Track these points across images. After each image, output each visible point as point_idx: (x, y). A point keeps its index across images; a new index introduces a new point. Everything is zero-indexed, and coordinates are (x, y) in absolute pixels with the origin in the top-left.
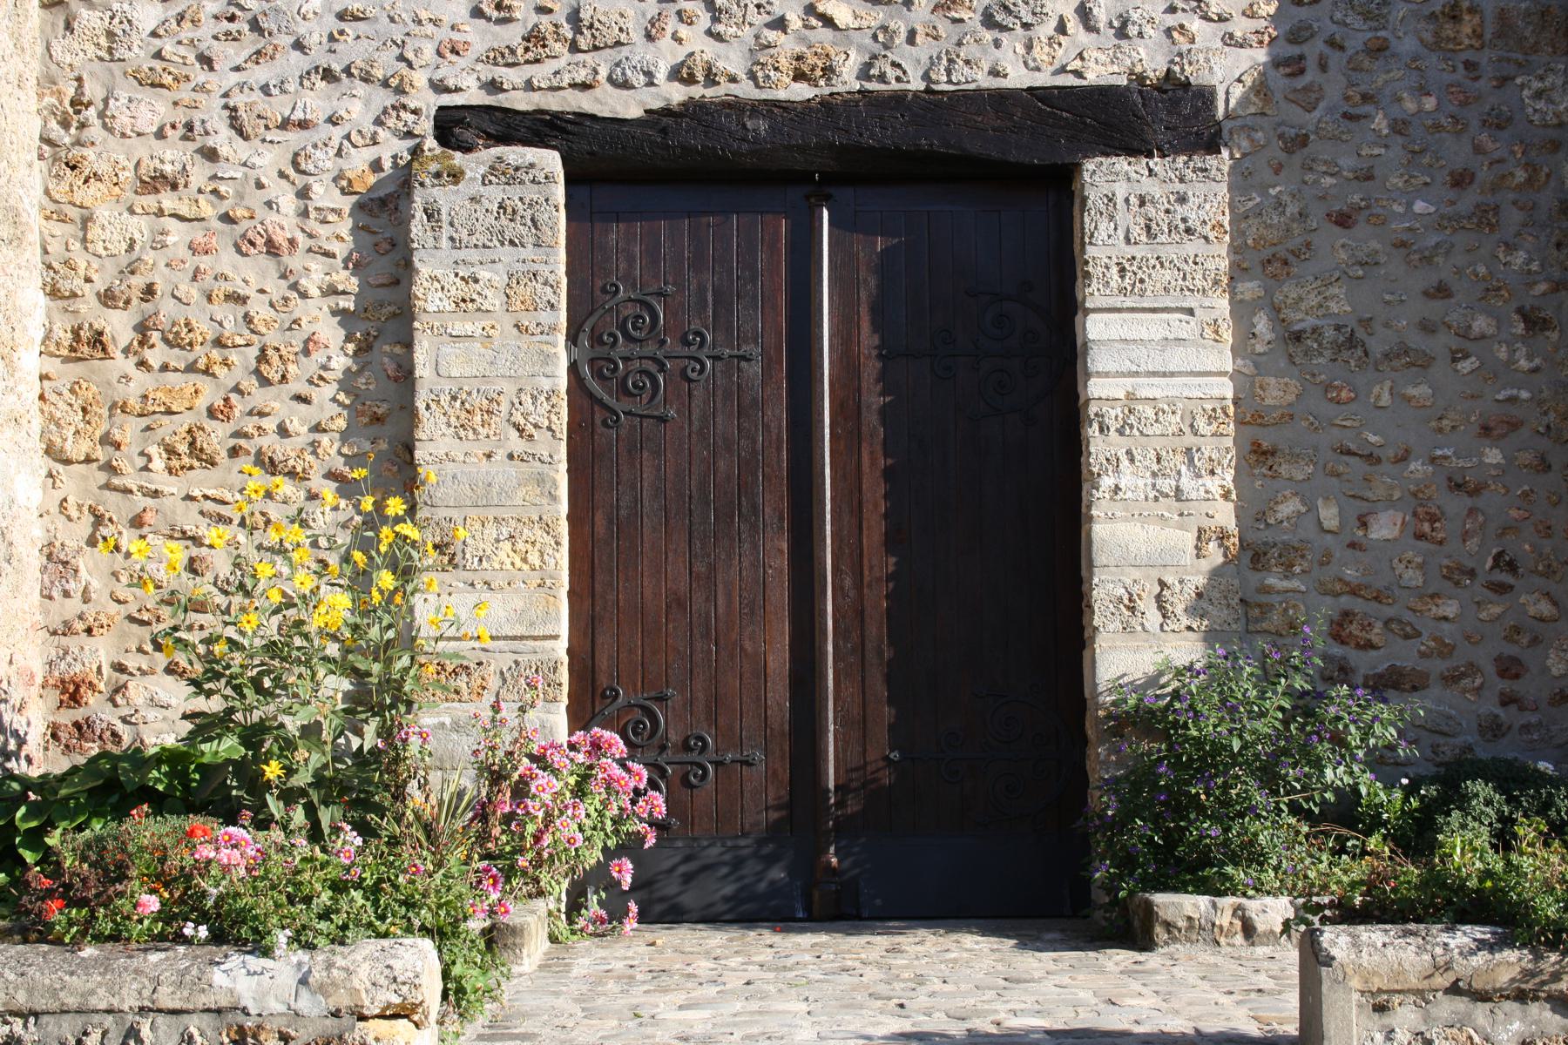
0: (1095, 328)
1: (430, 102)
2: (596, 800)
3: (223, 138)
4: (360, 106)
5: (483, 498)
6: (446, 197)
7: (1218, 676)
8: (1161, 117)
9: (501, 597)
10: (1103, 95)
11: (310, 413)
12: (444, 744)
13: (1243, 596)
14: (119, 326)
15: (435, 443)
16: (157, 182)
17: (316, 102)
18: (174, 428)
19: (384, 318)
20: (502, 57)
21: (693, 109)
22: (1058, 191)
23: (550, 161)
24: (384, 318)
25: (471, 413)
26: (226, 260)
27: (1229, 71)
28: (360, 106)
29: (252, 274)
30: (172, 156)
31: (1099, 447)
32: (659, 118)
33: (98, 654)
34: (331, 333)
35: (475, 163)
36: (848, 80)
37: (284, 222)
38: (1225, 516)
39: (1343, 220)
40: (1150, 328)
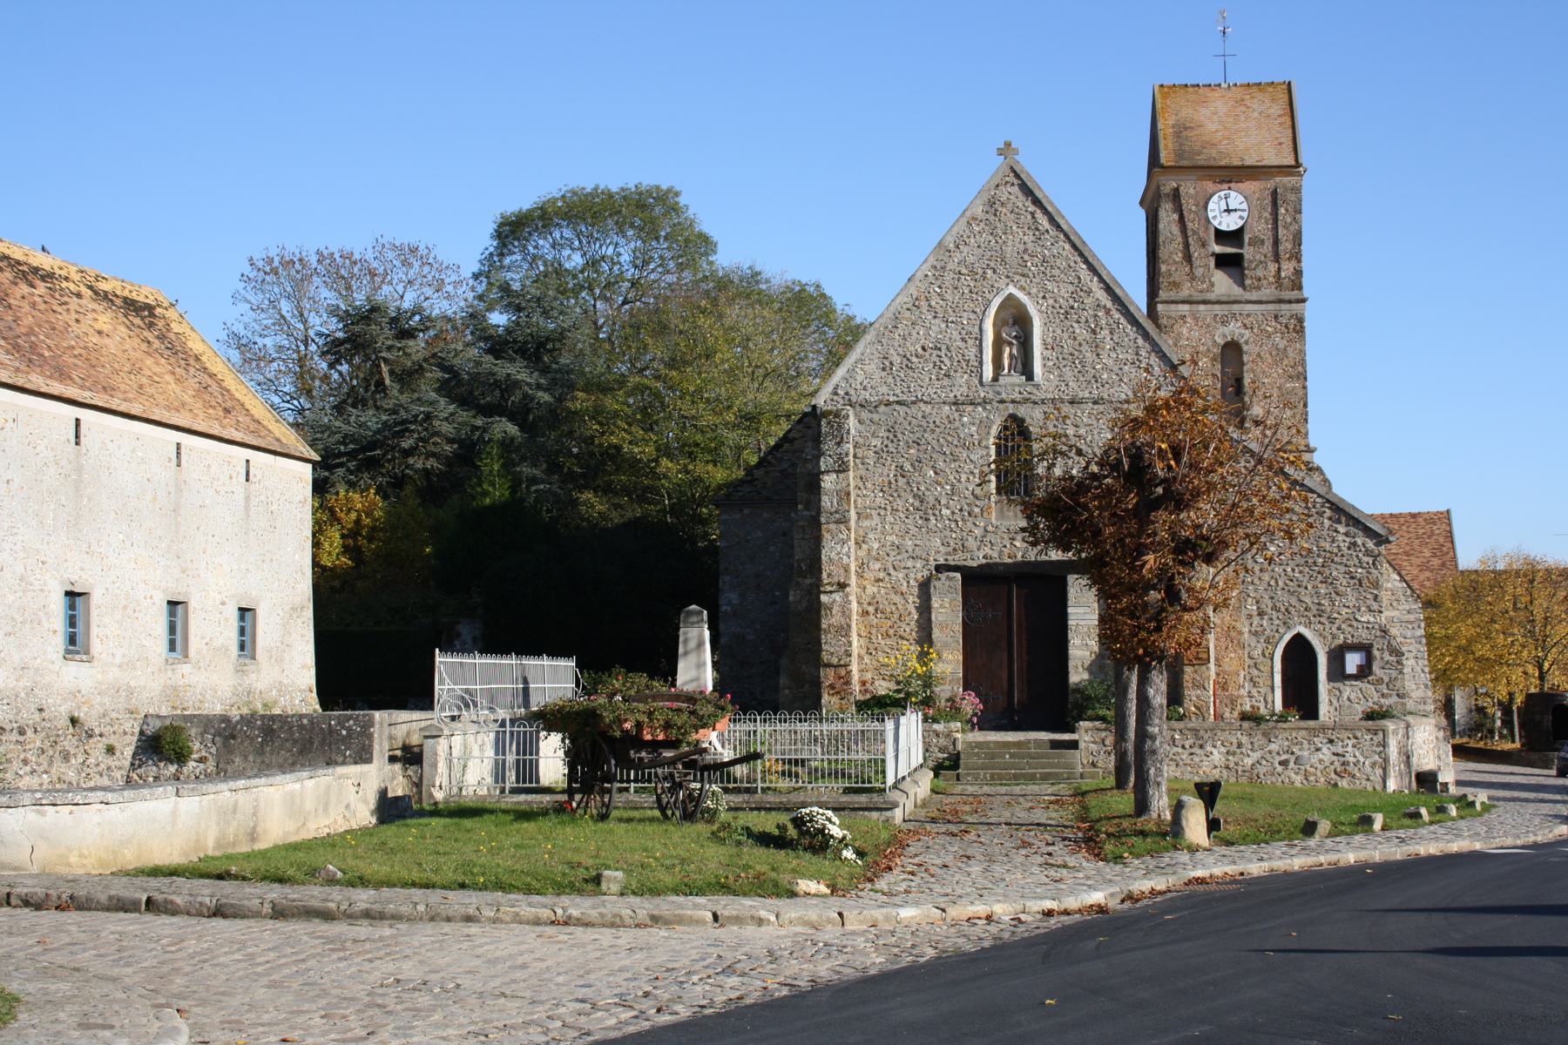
0: (1070, 610)
1: (933, 563)
2: (971, 704)
3: (892, 571)
4: (919, 565)
5: (946, 645)
6: (938, 584)
7: (1090, 682)
9: (949, 663)
11: (910, 628)
12: (943, 691)
13: (1096, 667)
14: (871, 609)
15: (936, 634)
16: (879, 580)
17: (910, 564)
18: (883, 630)
19: (925, 608)
20: (948, 554)
21: (987, 565)
23: (958, 575)
24: (925, 608)
25: (942, 627)
26: (893, 596)
28: (919, 565)
29: (897, 599)
30: (882, 575)
31: (1070, 635)
32: (980, 566)
33: (869, 676)
34: (914, 611)
35: (943, 576)
36: (1019, 558)
37: (904, 588)
38: (1096, 649)
40: (1081, 610)
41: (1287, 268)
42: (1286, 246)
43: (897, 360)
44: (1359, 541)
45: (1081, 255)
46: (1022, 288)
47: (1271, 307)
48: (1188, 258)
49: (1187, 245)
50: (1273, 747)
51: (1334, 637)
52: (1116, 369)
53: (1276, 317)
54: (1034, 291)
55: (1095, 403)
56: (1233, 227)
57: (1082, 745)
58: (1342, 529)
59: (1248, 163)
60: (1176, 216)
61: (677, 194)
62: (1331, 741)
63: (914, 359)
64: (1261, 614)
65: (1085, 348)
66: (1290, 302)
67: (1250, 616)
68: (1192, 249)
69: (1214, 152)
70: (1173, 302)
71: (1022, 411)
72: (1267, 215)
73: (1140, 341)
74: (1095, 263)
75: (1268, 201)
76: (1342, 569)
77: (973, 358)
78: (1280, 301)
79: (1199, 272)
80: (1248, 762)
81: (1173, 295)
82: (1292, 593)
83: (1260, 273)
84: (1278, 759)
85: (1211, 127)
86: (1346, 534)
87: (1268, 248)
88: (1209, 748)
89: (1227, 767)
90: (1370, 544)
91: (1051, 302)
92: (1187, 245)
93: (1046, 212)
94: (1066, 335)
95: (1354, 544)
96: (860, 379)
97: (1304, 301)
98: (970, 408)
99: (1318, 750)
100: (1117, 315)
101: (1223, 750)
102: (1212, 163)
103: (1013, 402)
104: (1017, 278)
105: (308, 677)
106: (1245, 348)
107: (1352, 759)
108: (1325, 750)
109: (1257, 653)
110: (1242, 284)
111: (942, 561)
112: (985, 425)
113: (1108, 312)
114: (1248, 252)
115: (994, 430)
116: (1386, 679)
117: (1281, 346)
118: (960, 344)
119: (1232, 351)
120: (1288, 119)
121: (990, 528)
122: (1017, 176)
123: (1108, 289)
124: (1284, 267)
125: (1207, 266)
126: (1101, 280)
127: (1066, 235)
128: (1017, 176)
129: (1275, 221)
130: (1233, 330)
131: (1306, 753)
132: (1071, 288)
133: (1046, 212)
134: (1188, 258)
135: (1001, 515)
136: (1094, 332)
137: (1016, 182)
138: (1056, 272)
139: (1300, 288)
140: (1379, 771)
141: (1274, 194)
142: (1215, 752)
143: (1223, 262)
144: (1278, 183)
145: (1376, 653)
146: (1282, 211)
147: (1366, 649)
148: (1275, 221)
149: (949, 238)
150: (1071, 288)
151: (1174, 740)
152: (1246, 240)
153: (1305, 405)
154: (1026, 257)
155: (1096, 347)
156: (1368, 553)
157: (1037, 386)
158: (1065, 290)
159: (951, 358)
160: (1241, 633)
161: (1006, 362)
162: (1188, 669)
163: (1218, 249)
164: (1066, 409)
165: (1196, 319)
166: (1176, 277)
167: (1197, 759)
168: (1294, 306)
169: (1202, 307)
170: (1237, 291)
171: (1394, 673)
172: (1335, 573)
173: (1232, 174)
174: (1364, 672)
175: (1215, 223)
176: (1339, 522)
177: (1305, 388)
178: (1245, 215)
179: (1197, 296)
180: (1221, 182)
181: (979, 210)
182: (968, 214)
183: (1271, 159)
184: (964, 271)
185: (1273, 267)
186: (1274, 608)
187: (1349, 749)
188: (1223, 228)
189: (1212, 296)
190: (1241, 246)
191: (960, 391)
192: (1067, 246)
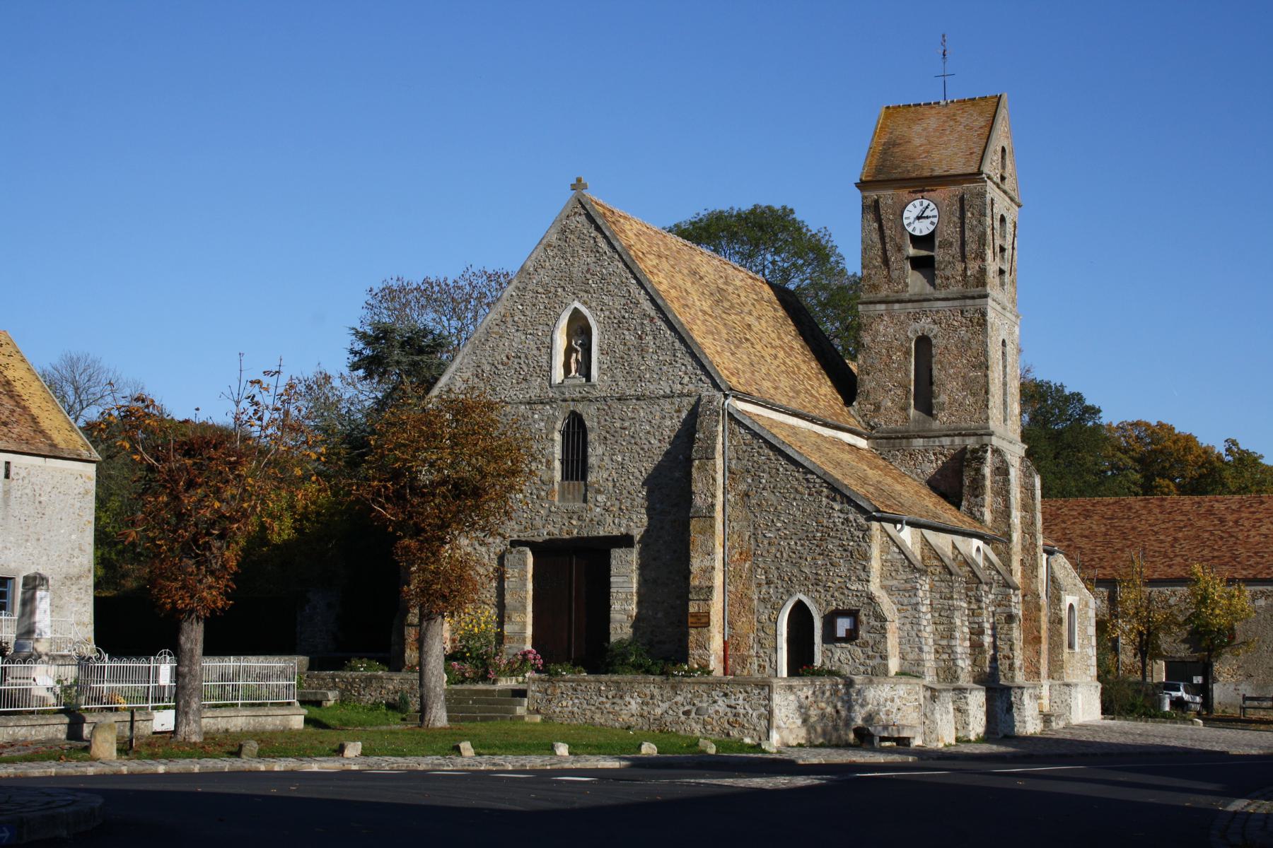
0: (612, 579)
3: (477, 546)
8: (625, 541)
10: (616, 537)
20: (520, 531)
27: (637, 533)
32: (545, 542)
39: (654, 559)
40: (621, 579)
41: (973, 267)
42: (972, 246)
43: (487, 368)
44: (851, 517)
45: (632, 272)
46: (585, 303)
47: (957, 303)
48: (886, 262)
49: (885, 251)
50: (679, 699)
51: (828, 603)
52: (656, 369)
53: (962, 312)
54: (594, 304)
55: (638, 399)
56: (925, 232)
57: (530, 694)
58: (837, 507)
59: (936, 173)
60: (876, 225)
61: (792, 211)
62: (726, 695)
63: (501, 367)
64: (769, 583)
65: (633, 352)
66: (973, 298)
67: (759, 585)
68: (889, 254)
69: (910, 166)
70: (871, 303)
71: (580, 408)
72: (956, 219)
73: (677, 344)
74: (642, 278)
75: (957, 207)
76: (837, 542)
77: (545, 364)
78: (965, 298)
79: (895, 274)
80: (658, 711)
81: (872, 296)
82: (794, 564)
83: (948, 272)
84: (682, 709)
85: (917, 142)
86: (841, 511)
87: (956, 249)
88: (627, 699)
89: (642, 716)
90: (862, 520)
91: (607, 313)
92: (885, 251)
93: (605, 237)
94: (618, 342)
95: (847, 520)
96: (458, 384)
97: (986, 296)
98: (540, 407)
99: (715, 702)
100: (659, 323)
101: (639, 700)
102: (905, 176)
103: (573, 400)
104: (582, 294)
105: (89, 632)
106: (934, 341)
107: (742, 711)
108: (720, 702)
109: (764, 617)
110: (932, 284)
111: (515, 537)
112: (551, 420)
113: (652, 319)
114: (938, 254)
115: (559, 425)
116: (871, 642)
117: (966, 338)
118: (535, 352)
119: (924, 343)
120: (987, 130)
121: (553, 509)
122: (583, 207)
123: (653, 301)
125: (902, 269)
126: (647, 293)
127: (620, 255)
128: (583, 207)
130: (925, 325)
131: (705, 705)
132: (623, 301)
133: (605, 237)
135: (563, 497)
136: (640, 338)
137: (583, 212)
138: (611, 288)
139: (984, 285)
140: (764, 723)
141: (962, 200)
142: (633, 702)
143: (917, 263)
144: (963, 188)
146: (969, 215)
147: (853, 614)
148: (963, 224)
149: (529, 263)
150: (623, 301)
151: (600, 690)
152: (937, 243)
153: (987, 392)
154: (588, 276)
155: (642, 351)
156: (859, 528)
157: (593, 386)
158: (618, 303)
159: (528, 365)
160: (751, 600)
161: (573, 367)
162: (692, 631)
163: (911, 251)
164: (616, 405)
165: (892, 317)
166: (875, 280)
167: (617, 708)
168: (978, 301)
169: (897, 306)
170: (929, 289)
171: (878, 637)
172: (830, 546)
173: (923, 184)
174: (852, 636)
175: (910, 229)
176: (834, 500)
177: (986, 376)
178: (935, 220)
179: (893, 296)
180: (915, 192)
181: (554, 238)
182: (544, 242)
183: (959, 168)
184: (541, 290)
185: (960, 267)
186: (780, 578)
187: (741, 702)
188: (917, 233)
189: (906, 296)
190: (932, 250)
191: (534, 393)
192: (621, 265)
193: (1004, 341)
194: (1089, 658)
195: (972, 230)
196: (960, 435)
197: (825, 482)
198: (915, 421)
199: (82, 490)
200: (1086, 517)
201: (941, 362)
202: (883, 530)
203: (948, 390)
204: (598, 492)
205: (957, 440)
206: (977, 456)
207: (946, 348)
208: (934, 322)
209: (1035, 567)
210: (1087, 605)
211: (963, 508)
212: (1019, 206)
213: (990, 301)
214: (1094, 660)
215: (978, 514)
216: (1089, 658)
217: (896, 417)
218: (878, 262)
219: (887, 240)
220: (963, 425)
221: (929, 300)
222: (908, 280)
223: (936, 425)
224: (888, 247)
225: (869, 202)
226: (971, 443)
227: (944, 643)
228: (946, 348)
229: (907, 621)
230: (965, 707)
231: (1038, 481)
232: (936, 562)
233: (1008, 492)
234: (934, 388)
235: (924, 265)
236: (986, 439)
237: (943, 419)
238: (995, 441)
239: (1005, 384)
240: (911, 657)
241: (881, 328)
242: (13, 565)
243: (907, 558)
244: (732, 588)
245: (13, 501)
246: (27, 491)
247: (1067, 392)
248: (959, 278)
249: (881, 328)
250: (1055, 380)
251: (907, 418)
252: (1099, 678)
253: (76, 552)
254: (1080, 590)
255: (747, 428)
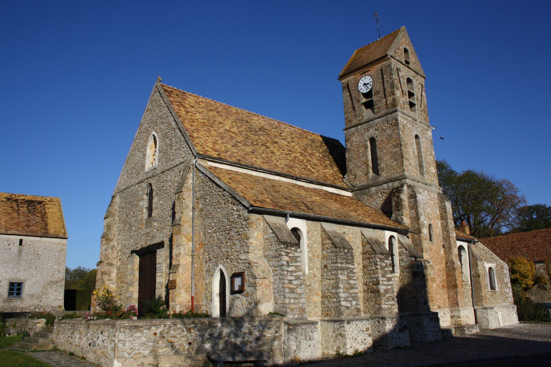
0: (157, 266)
22: (155, 252)
42: (388, 90)
47: (384, 118)
48: (354, 108)
49: (353, 104)
66: (391, 113)
75: (380, 74)
79: (357, 113)
83: (379, 106)
87: (382, 94)
92: (353, 104)
97: (396, 111)
105: (62, 303)
106: (376, 139)
124: (388, 99)
129: (383, 81)
130: (372, 132)
134: (354, 108)
141: (382, 70)
145: (246, 277)
146: (385, 76)
147: (240, 275)
148: (383, 81)
152: (373, 94)
163: (364, 100)
165: (358, 133)
169: (359, 127)
175: (362, 91)
177: (401, 149)
185: (384, 101)
188: (365, 92)
193: (417, 137)
194: (508, 293)
195: (387, 83)
196: (391, 181)
197: (230, 194)
198: (372, 179)
199: (60, 249)
200: (534, 238)
201: (380, 148)
202: (265, 220)
203: (385, 161)
204: (155, 221)
205: (390, 184)
206: (398, 190)
207: (382, 141)
208: (376, 130)
209: (450, 248)
210: (502, 267)
211: (392, 218)
212: (424, 78)
213: (399, 113)
214: (511, 294)
215: (400, 220)
216: (508, 293)
217: (363, 179)
218: (351, 110)
219: (353, 99)
220: (393, 176)
221: (372, 120)
222: (364, 114)
223: (381, 179)
224: (354, 102)
225: (345, 85)
226: (396, 184)
227: (334, 291)
228: (382, 141)
229: (277, 277)
230: (344, 333)
231: (448, 205)
232: (328, 241)
233: (417, 206)
234: (379, 161)
235: (369, 105)
236: (403, 180)
237: (384, 175)
238: (408, 181)
239: (420, 156)
240: (279, 302)
241: (354, 139)
242: (22, 278)
243: (276, 236)
244: (196, 265)
245: (23, 254)
246: (32, 250)
247: (547, 207)
248: (385, 106)
249: (354, 139)
250: (542, 203)
251: (368, 179)
252: (516, 302)
253: (56, 272)
254: (496, 261)
255: (203, 173)
